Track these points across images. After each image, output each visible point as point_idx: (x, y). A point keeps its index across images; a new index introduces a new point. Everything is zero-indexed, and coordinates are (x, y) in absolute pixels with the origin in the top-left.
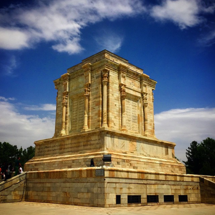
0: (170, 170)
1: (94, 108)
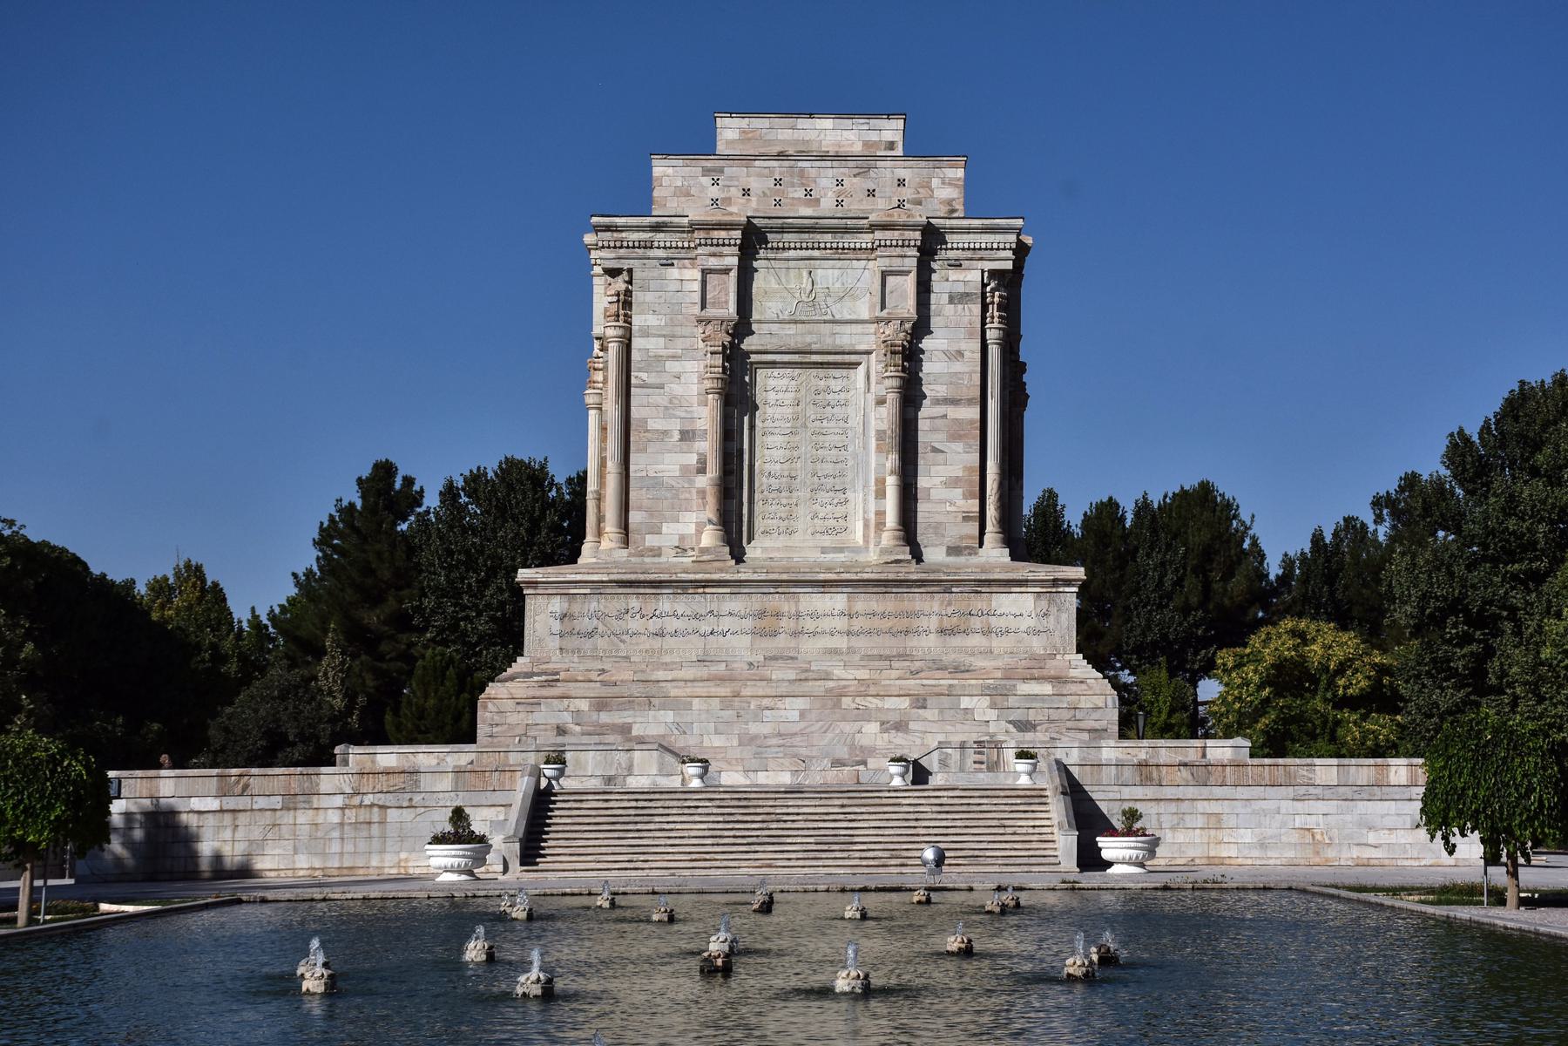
1: (935, 450)
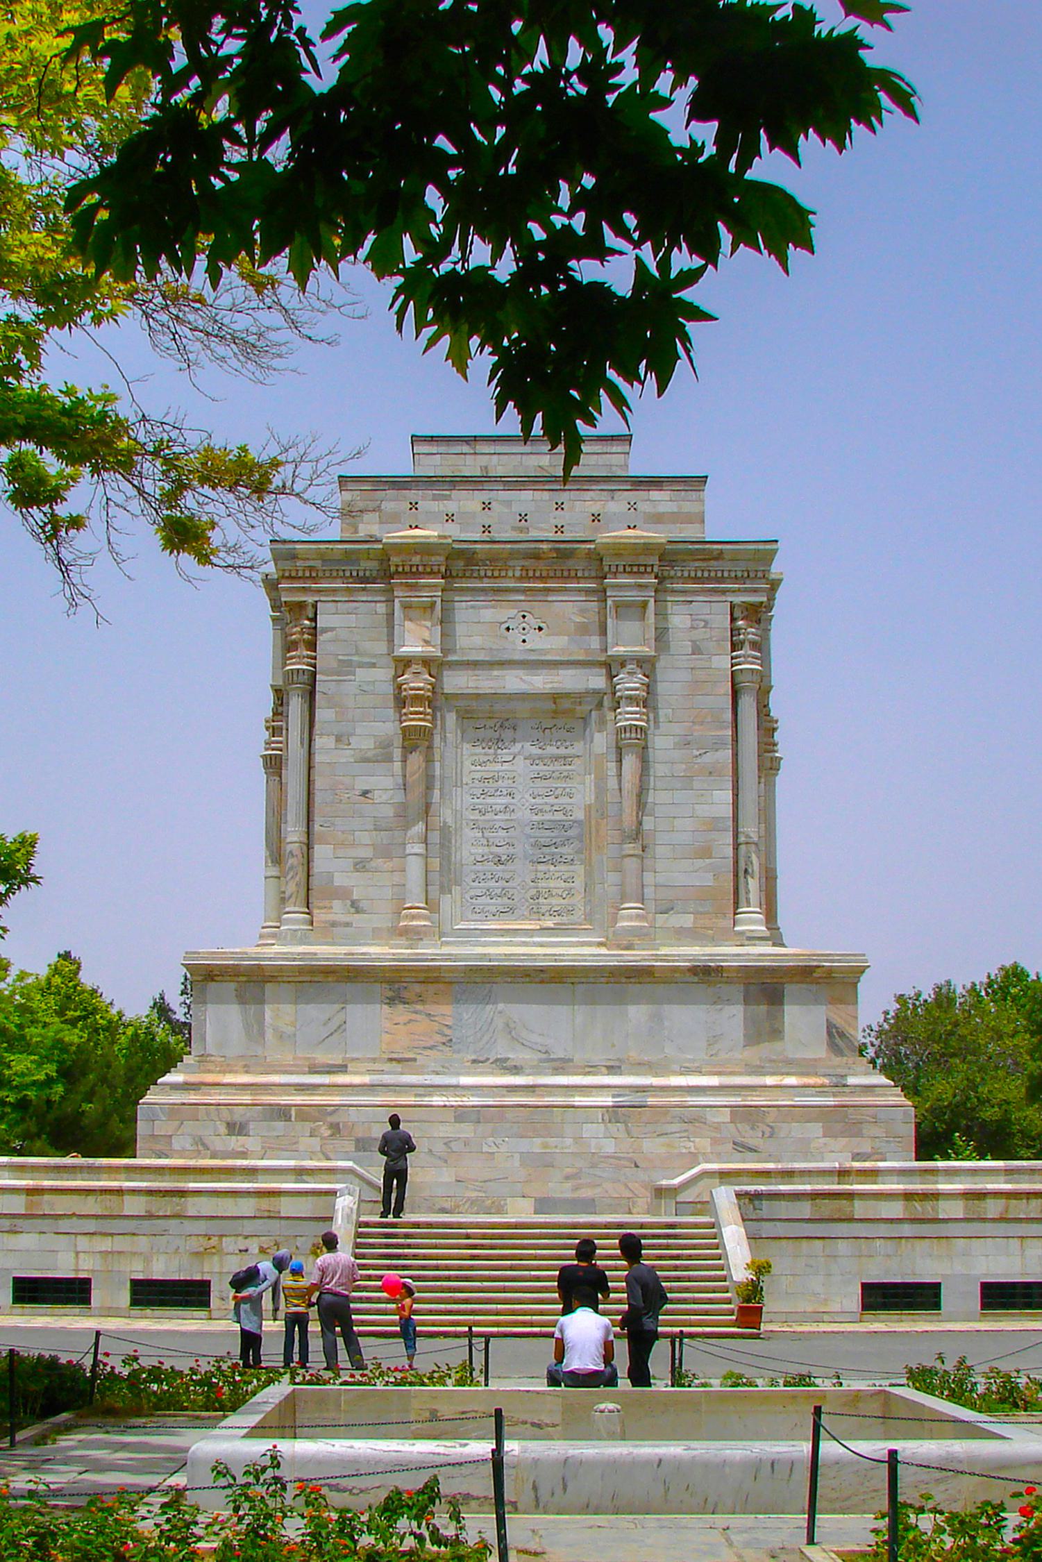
0: (715, 1141)
